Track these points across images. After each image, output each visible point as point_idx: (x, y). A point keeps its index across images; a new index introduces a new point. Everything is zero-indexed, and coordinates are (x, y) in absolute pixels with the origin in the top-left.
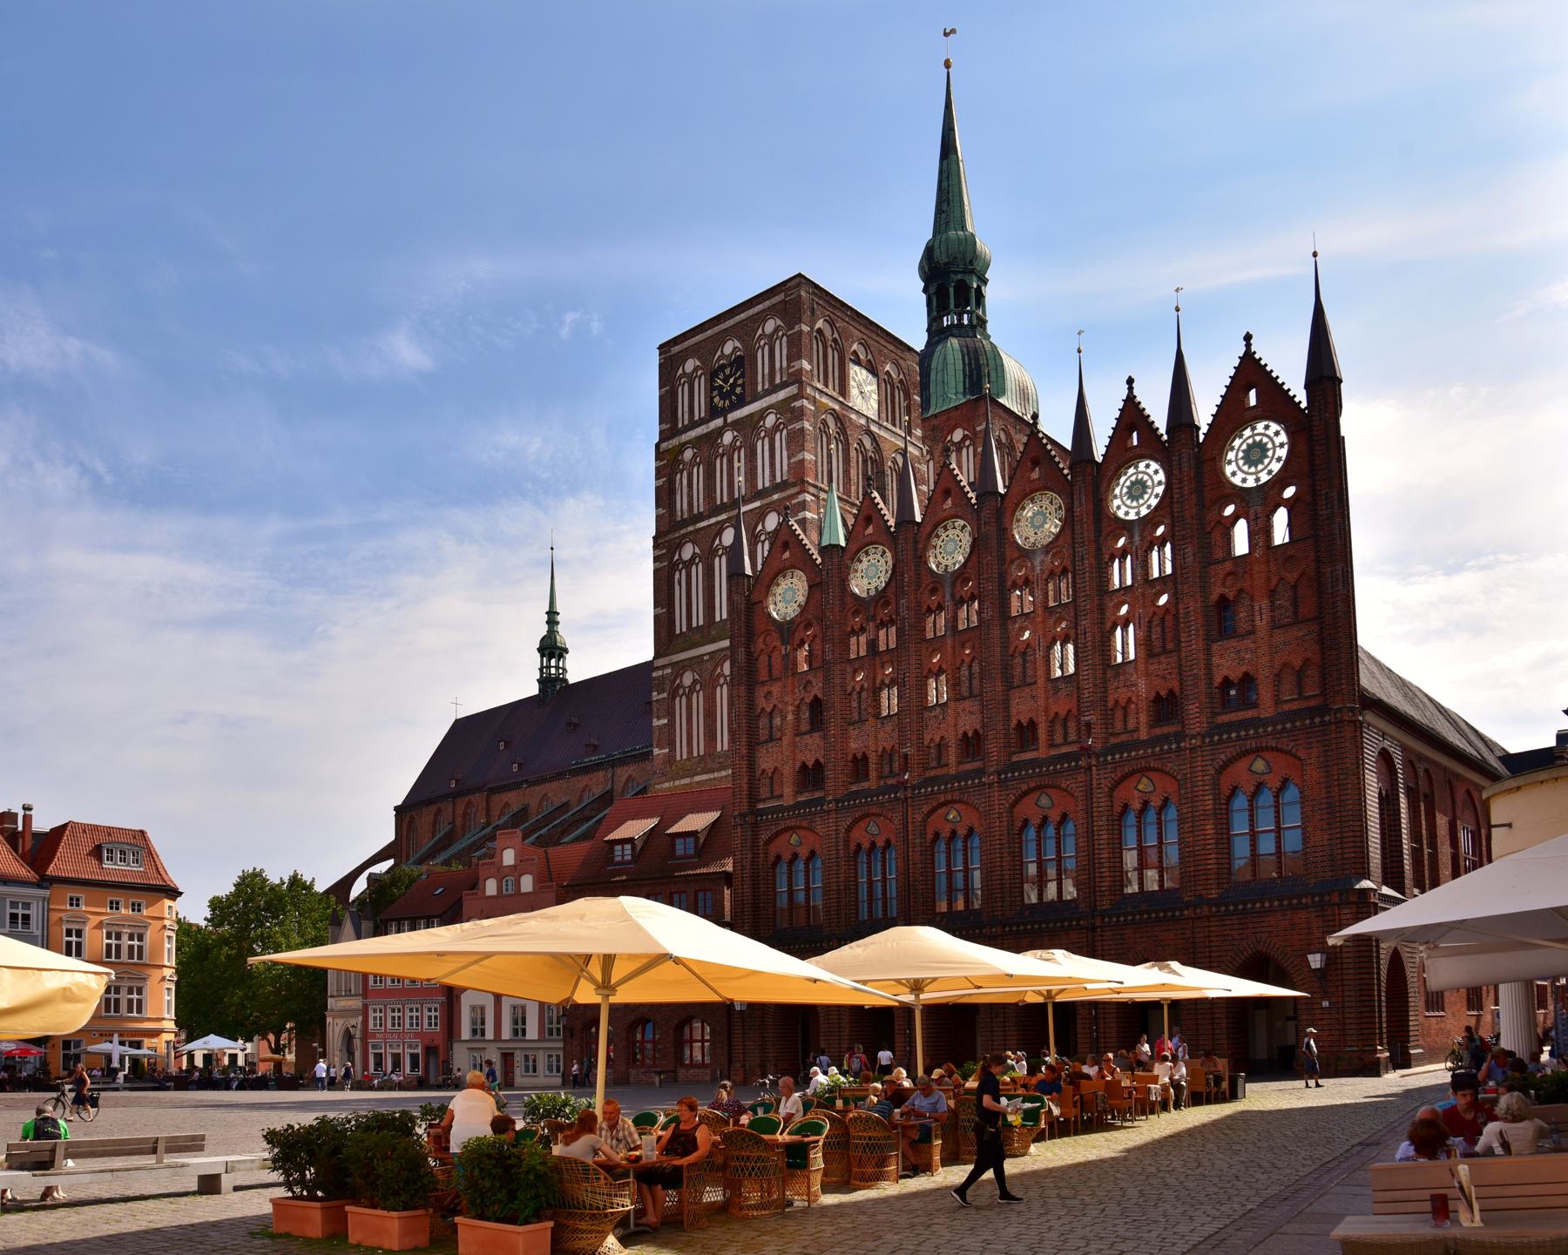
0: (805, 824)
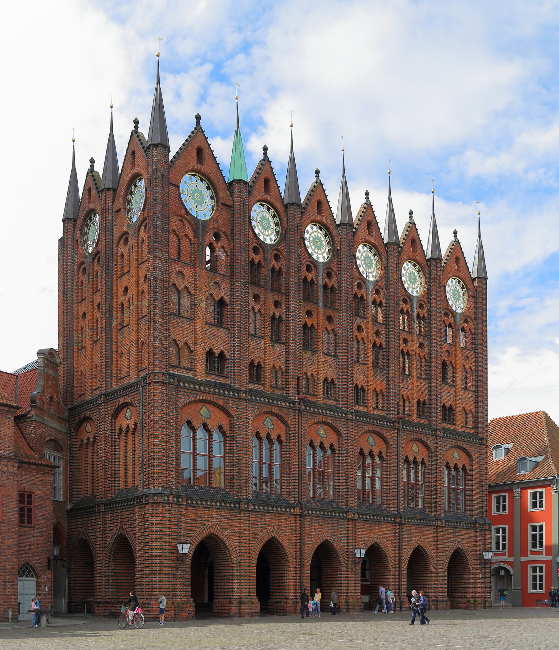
0: (220, 402)
